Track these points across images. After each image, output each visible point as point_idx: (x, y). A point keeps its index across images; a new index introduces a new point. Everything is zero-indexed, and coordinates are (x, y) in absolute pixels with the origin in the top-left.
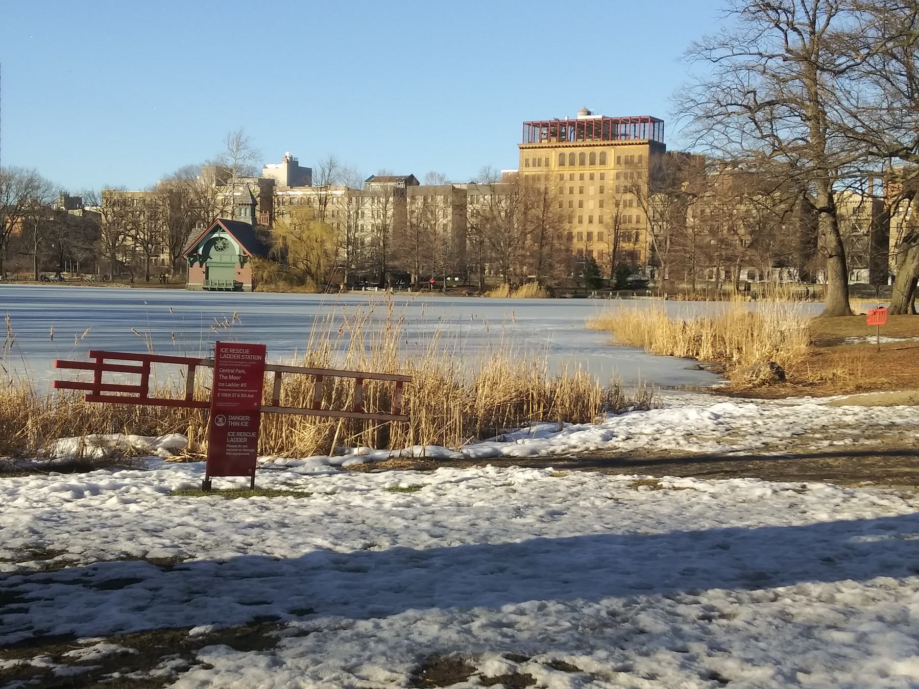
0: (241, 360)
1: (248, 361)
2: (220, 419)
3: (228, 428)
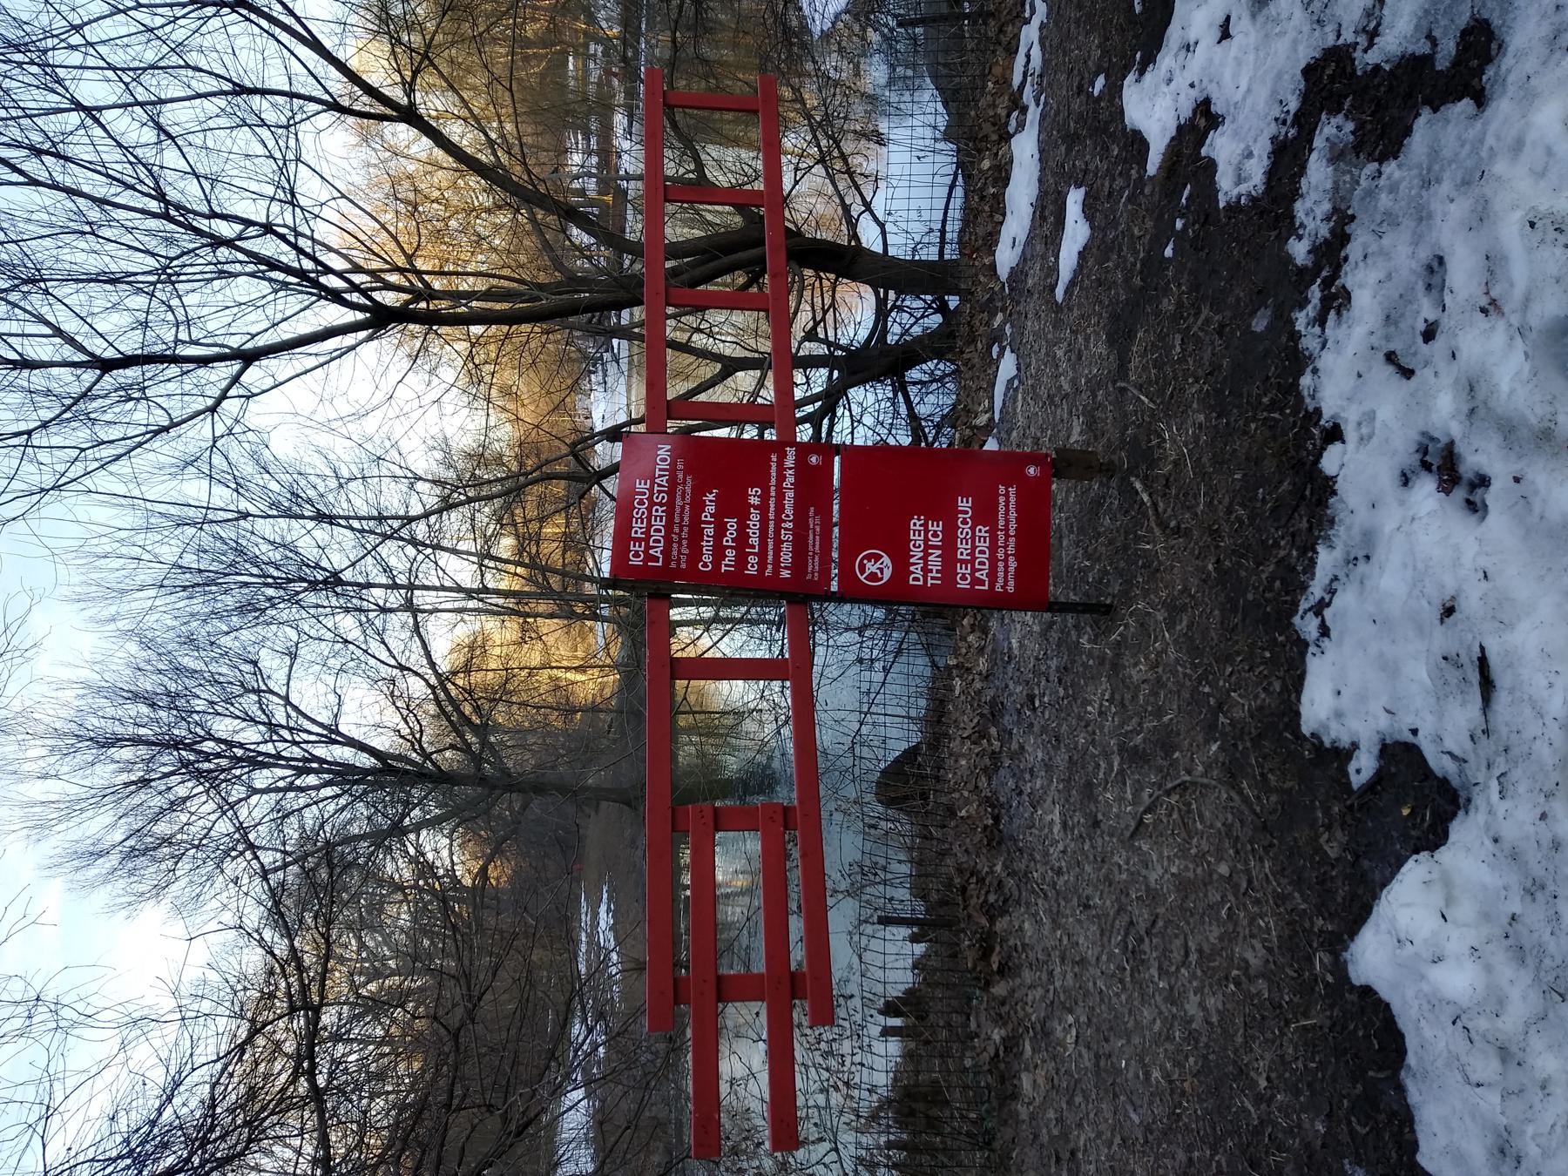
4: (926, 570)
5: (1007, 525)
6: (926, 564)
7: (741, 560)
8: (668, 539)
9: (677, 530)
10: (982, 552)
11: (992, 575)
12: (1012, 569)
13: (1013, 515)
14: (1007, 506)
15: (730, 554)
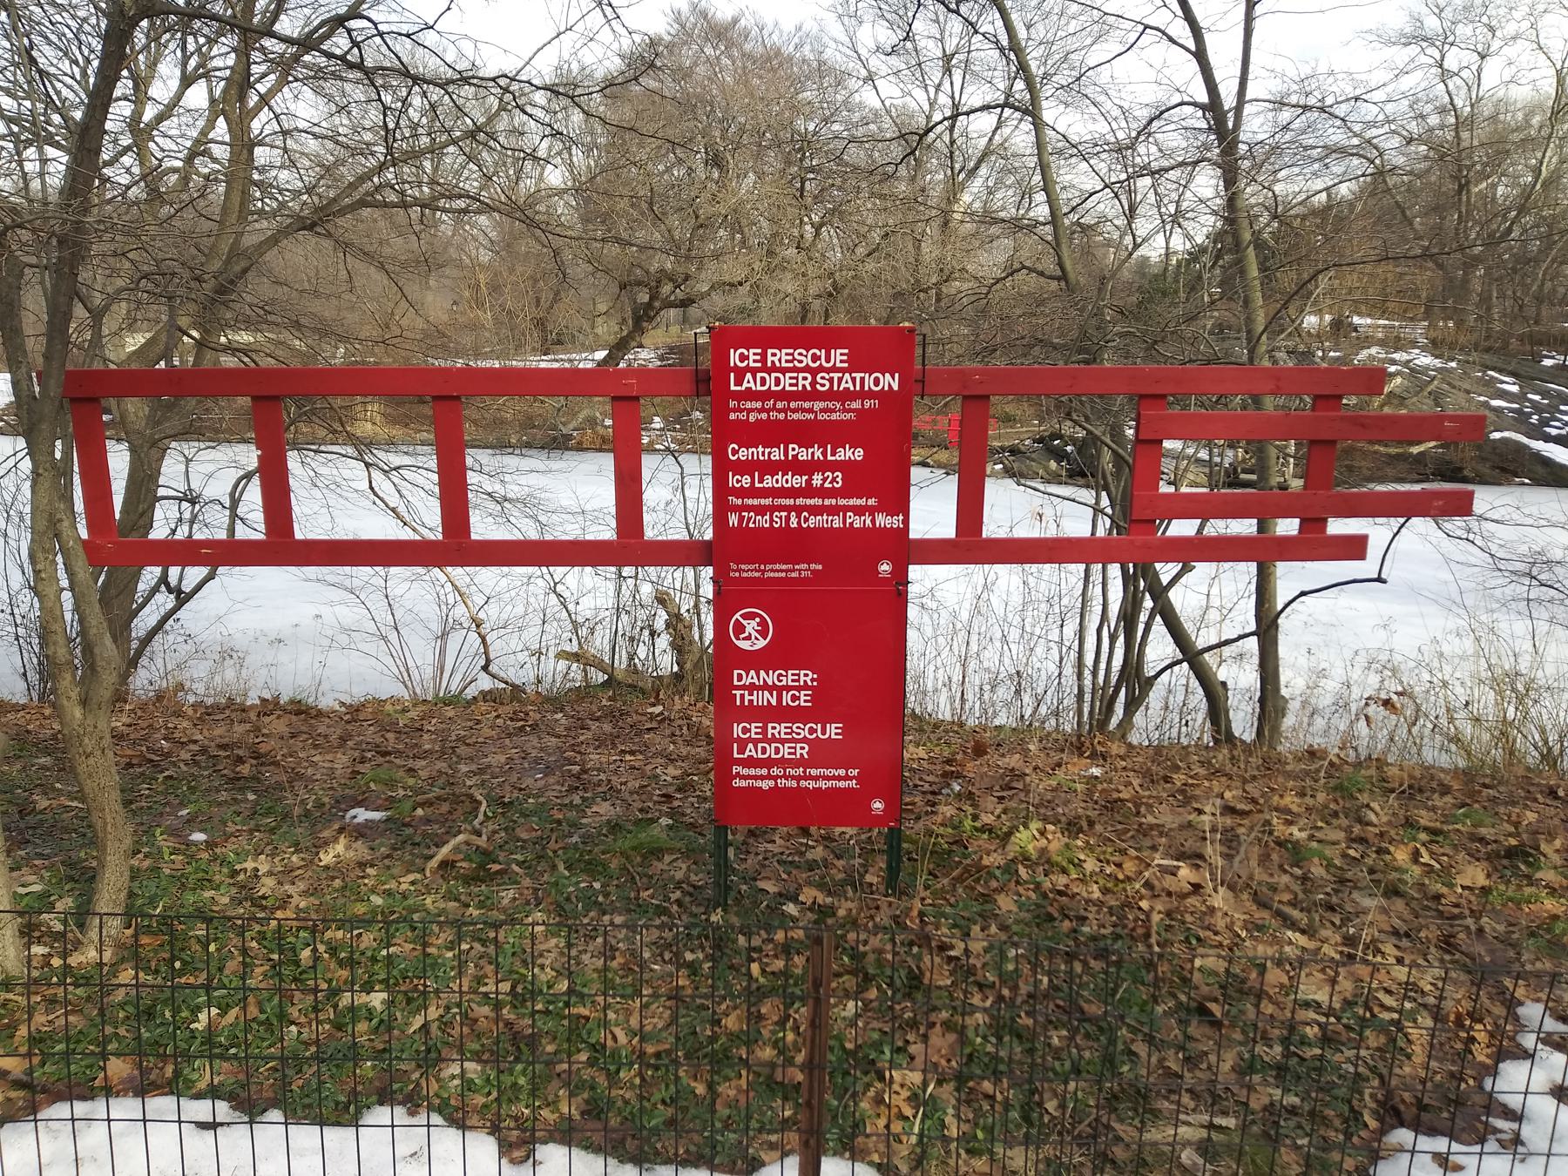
0: (814, 395)
1: (846, 396)
2: (751, 626)
4: (751, 688)
5: (811, 778)
6: (759, 688)
8: (768, 395)
9: (780, 405)
10: (777, 751)
11: (751, 762)
12: (759, 784)
13: (823, 785)
14: (834, 778)
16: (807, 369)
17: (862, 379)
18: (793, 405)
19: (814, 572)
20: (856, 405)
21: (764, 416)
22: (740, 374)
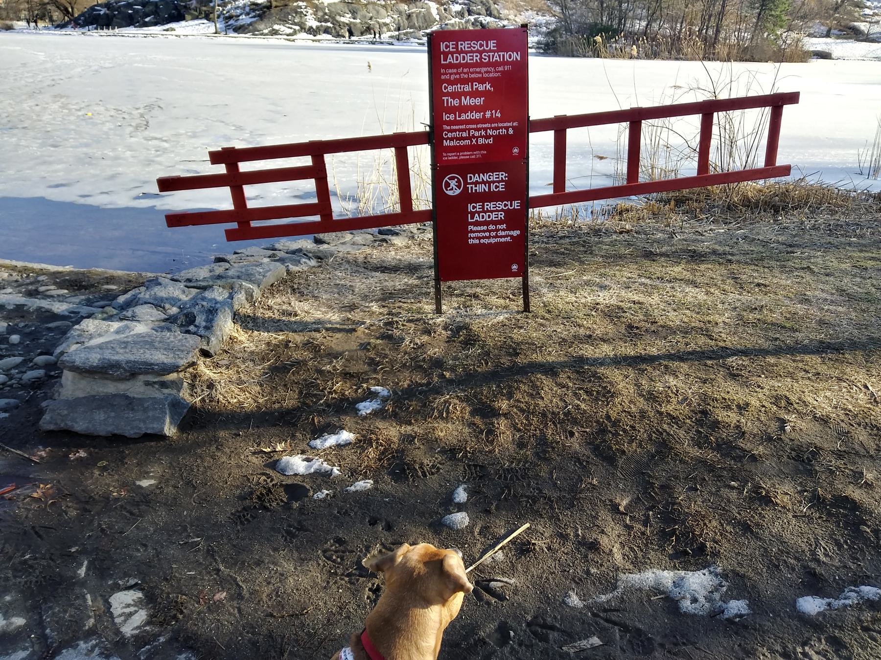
1: (495, 64)
2: (453, 183)
3: (468, 197)
7: (451, 110)
9: (465, 70)
15: (456, 102)
16: (477, 51)
17: (504, 56)
18: (471, 70)
19: (482, 155)
20: (501, 69)
21: (458, 76)
22: (446, 55)
